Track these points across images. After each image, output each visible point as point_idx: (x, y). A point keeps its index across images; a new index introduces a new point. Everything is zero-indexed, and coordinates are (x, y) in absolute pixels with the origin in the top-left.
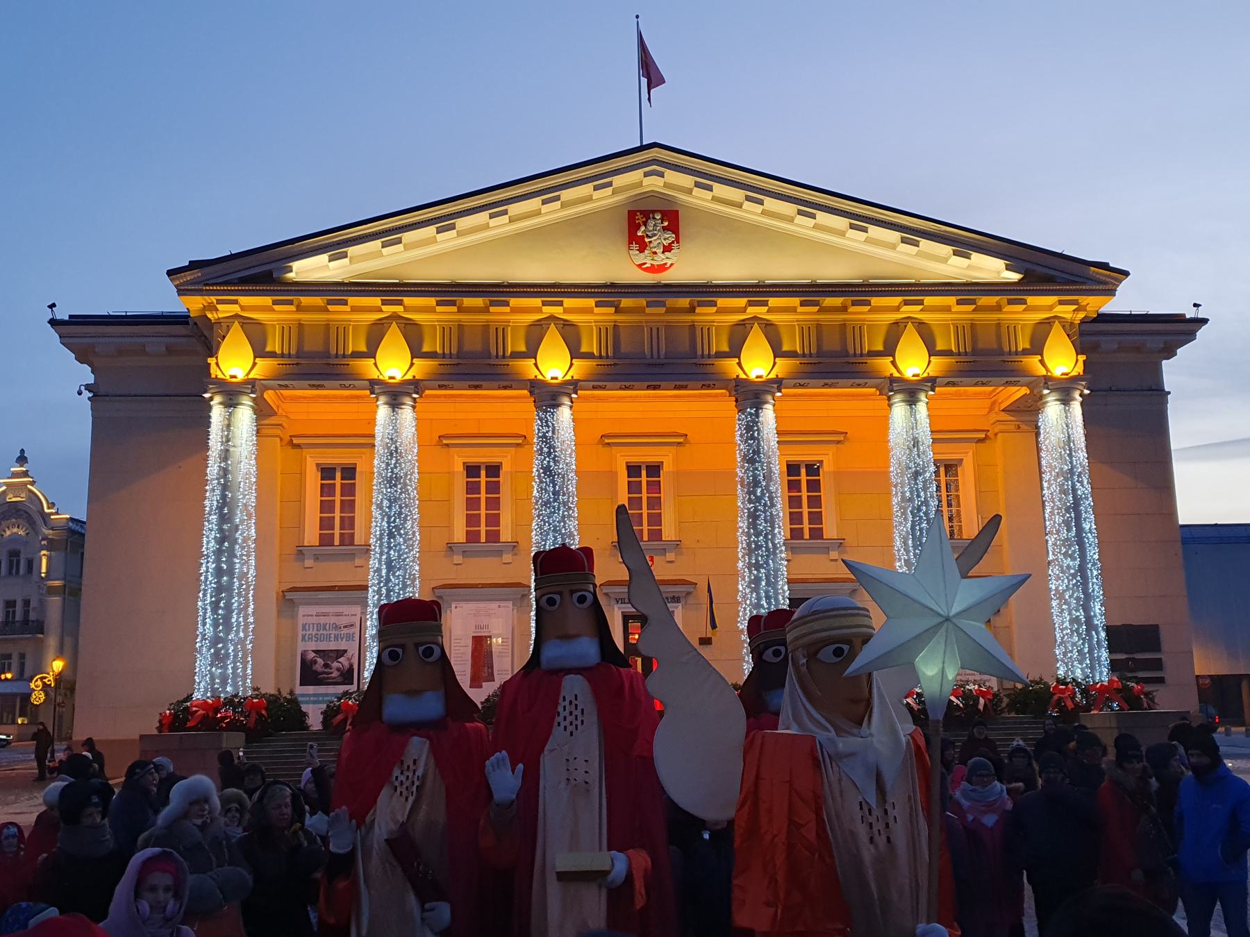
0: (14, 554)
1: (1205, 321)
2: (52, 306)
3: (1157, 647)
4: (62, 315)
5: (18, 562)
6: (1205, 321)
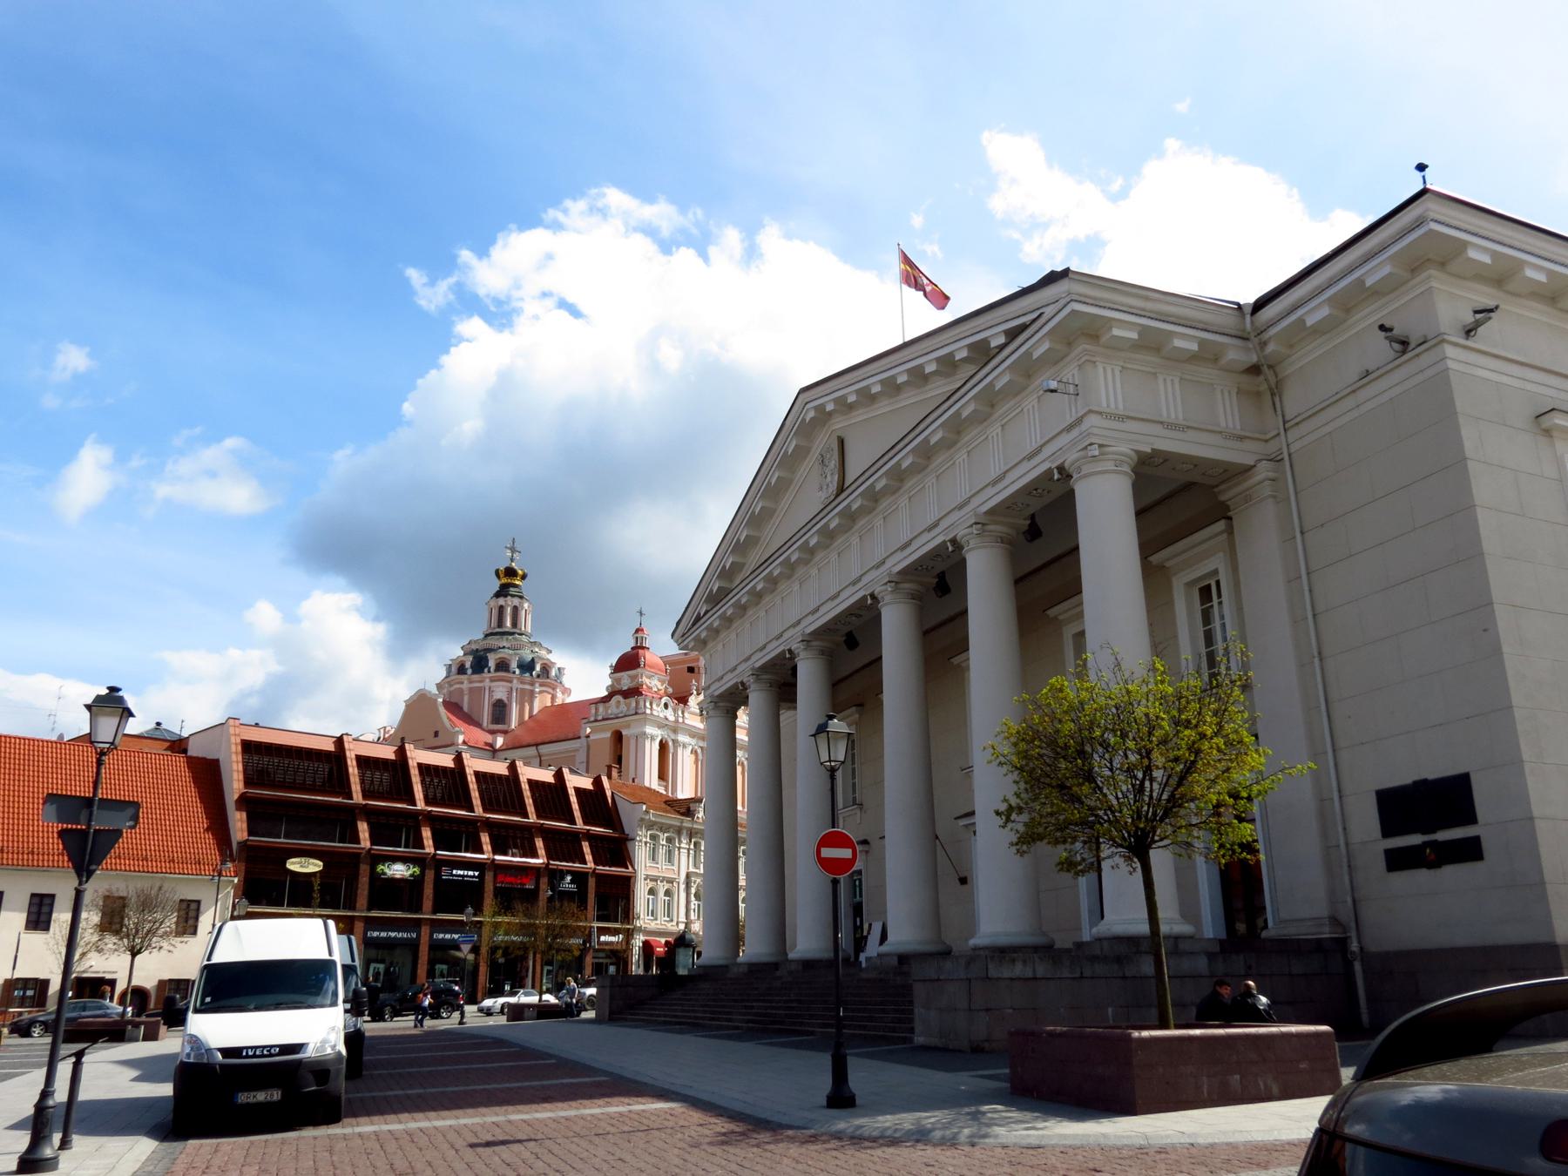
3: (1472, 819)
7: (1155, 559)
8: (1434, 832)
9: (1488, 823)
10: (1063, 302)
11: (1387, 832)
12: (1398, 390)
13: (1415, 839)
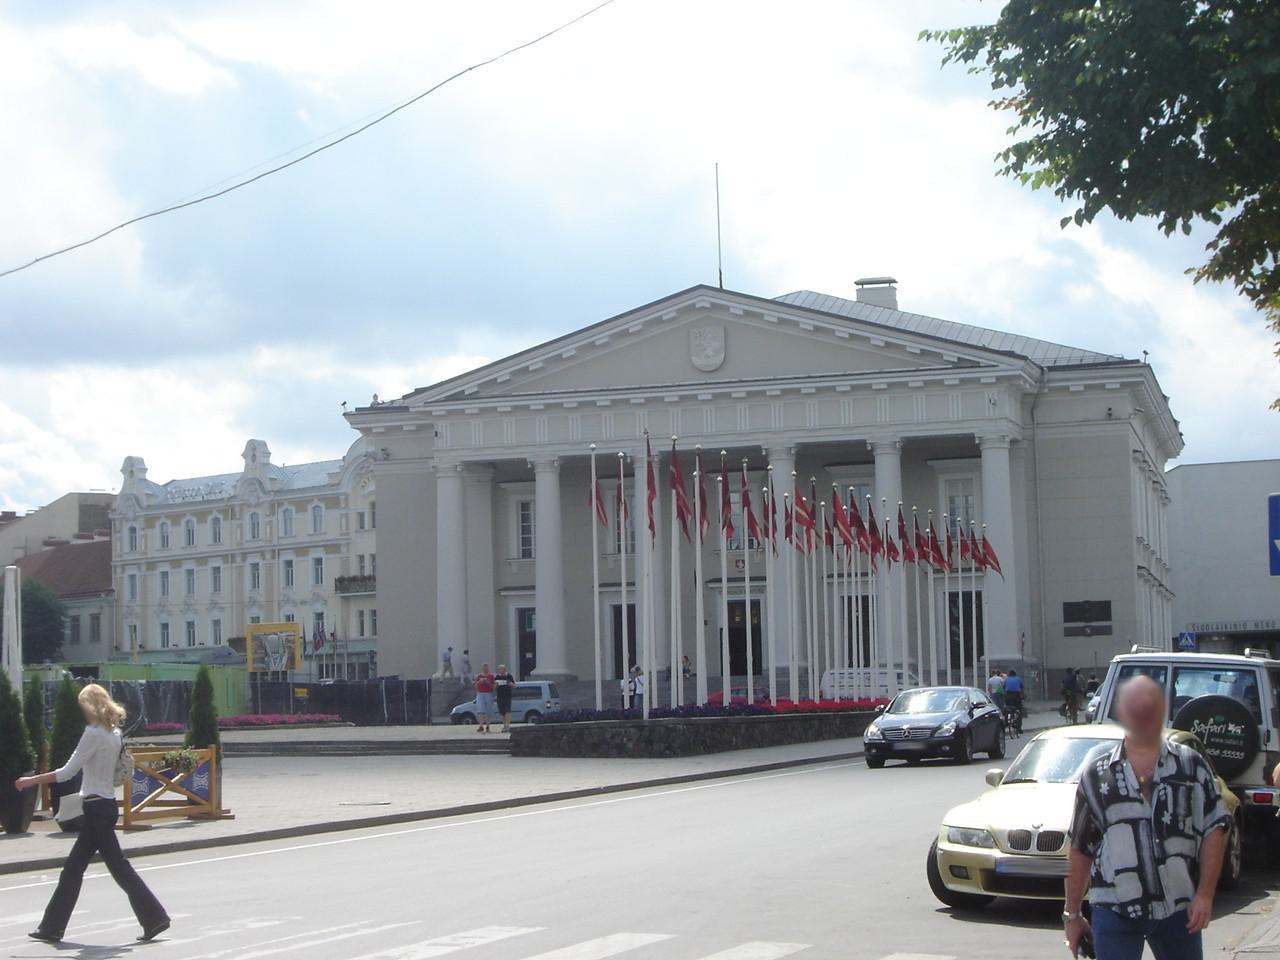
2: (345, 403)
3: (1110, 619)
4: (351, 408)
8: (1091, 621)
10: (1009, 367)
11: (1065, 621)
13: (1082, 624)
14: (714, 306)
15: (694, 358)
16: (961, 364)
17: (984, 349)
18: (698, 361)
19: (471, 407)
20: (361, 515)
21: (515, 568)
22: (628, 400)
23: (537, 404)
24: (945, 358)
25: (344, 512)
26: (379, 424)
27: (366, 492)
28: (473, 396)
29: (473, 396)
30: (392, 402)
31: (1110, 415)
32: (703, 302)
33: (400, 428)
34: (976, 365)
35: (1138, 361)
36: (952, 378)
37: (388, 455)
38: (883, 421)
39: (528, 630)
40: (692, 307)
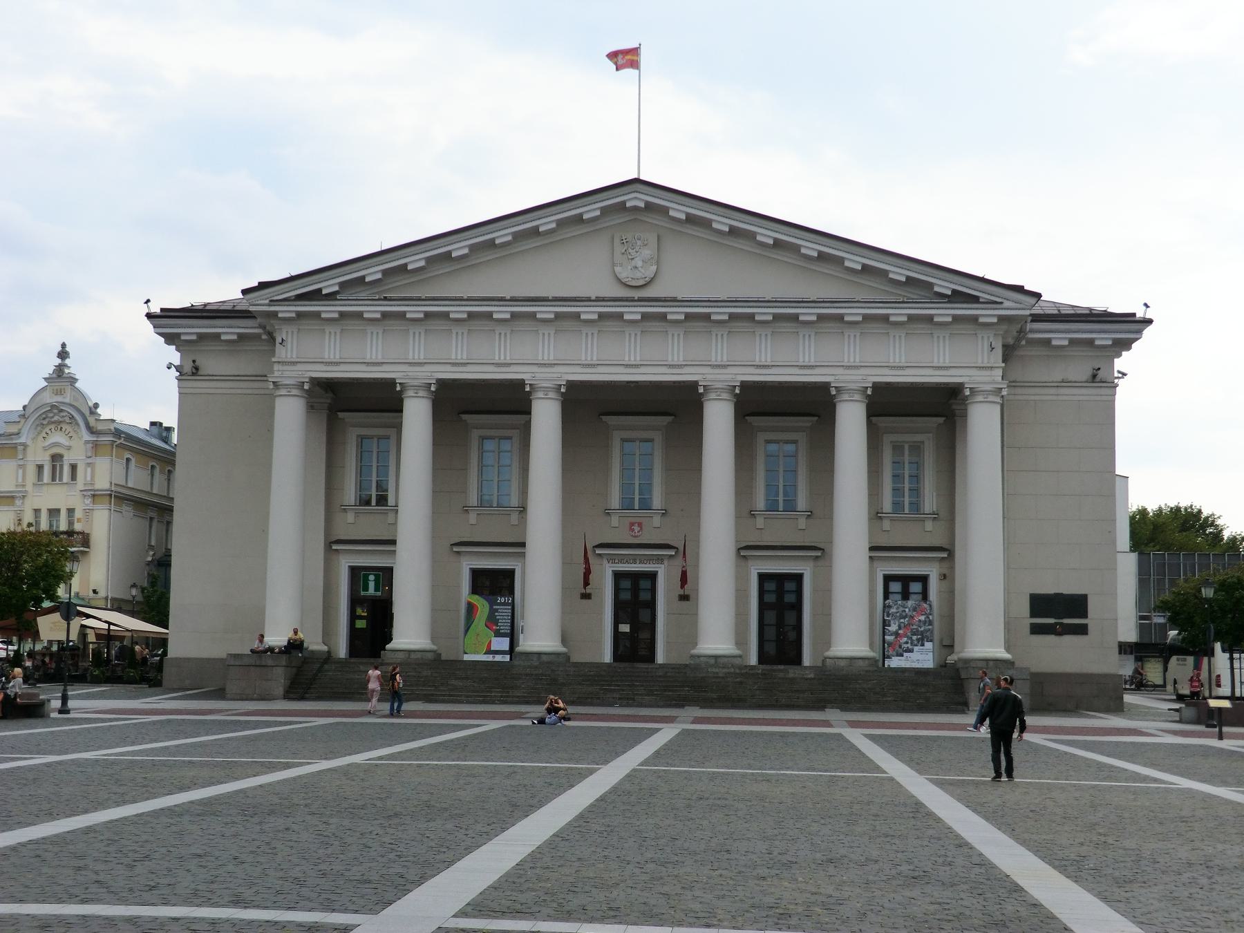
0: (56, 458)
1: (1150, 322)
5: (62, 466)
6: (1150, 322)
7: (874, 419)
9: (1091, 621)
11: (1033, 615)
12: (1081, 398)
13: (1052, 621)
14: (649, 207)
15: (617, 269)
16: (957, 297)
17: (982, 280)
18: (624, 273)
19: (329, 310)
20: (40, 468)
21: (350, 517)
22: (534, 314)
23: (414, 311)
24: (936, 289)
25: (21, 463)
26: (189, 330)
27: (47, 443)
28: (331, 296)
29: (331, 296)
30: (205, 305)
31: (1094, 376)
32: (635, 200)
33: (217, 336)
34: (975, 299)
35: (1134, 315)
36: (944, 313)
37: (197, 369)
38: (852, 364)
39: (362, 593)
40: (622, 207)
